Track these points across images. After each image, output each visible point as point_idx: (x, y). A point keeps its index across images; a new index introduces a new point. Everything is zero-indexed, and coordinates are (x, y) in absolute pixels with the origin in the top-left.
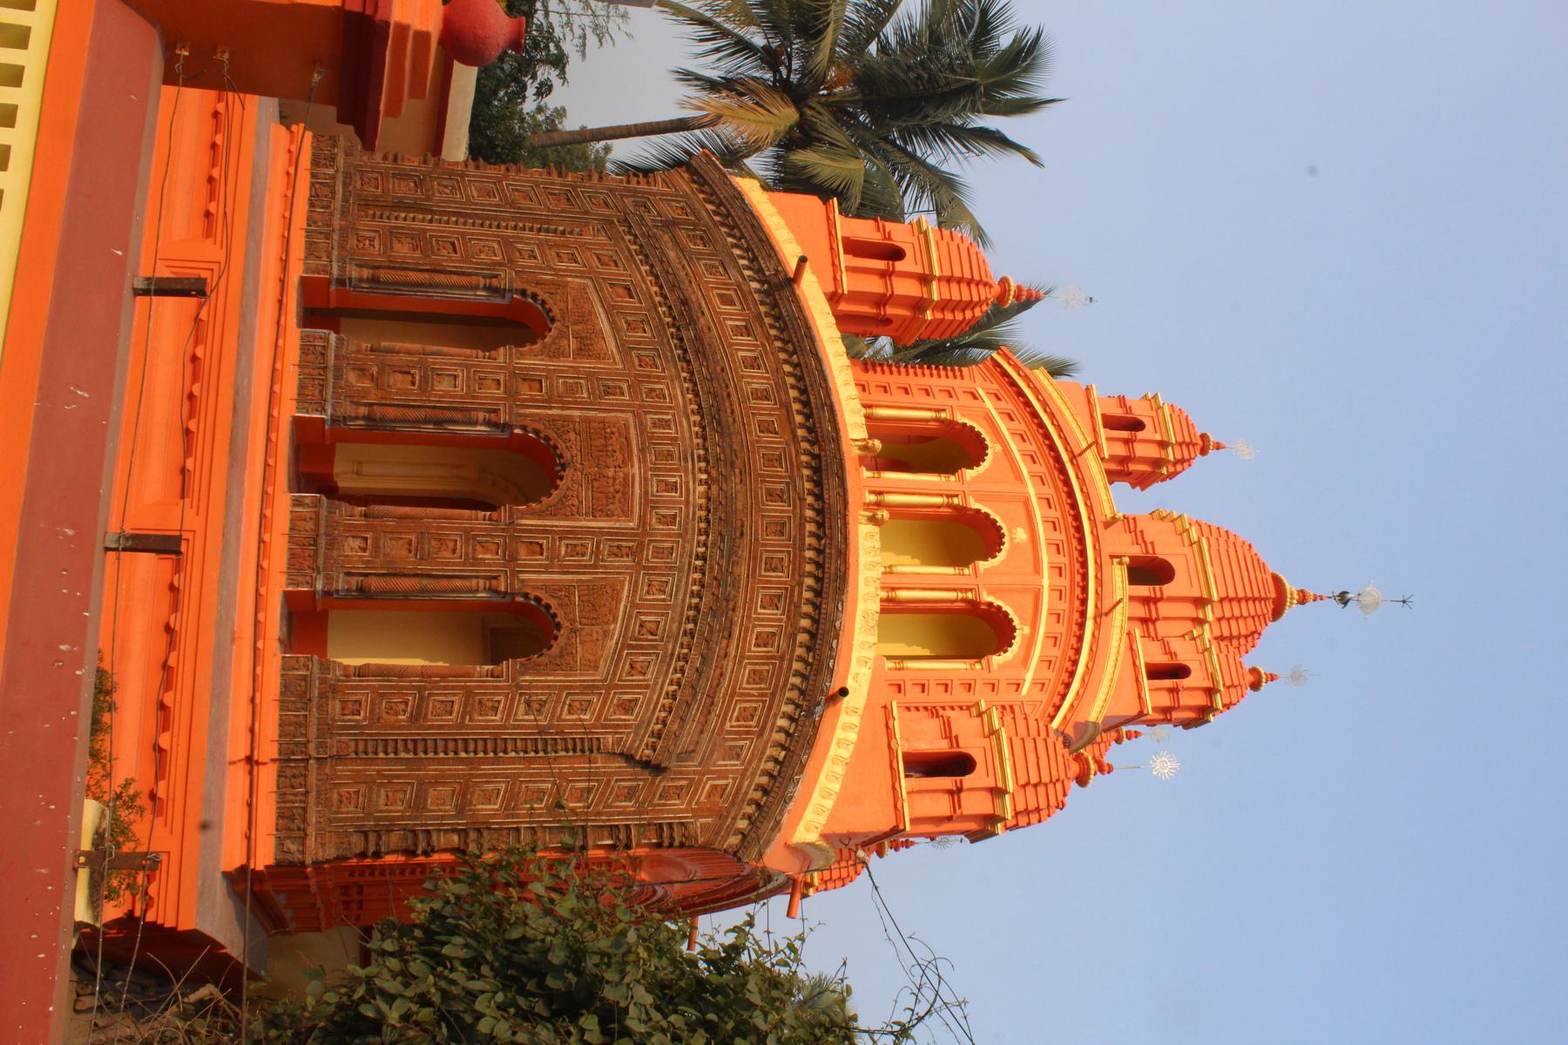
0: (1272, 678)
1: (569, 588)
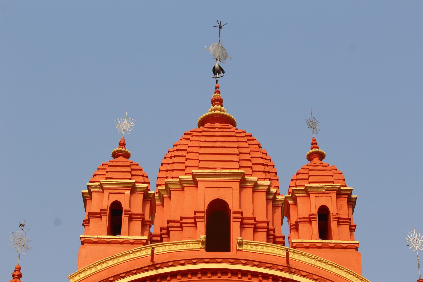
0: (314, 144)
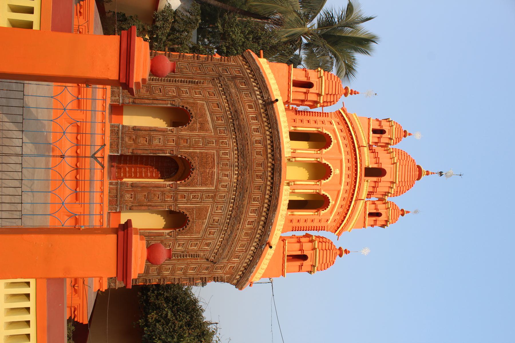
0: (408, 212)
1: (193, 209)
